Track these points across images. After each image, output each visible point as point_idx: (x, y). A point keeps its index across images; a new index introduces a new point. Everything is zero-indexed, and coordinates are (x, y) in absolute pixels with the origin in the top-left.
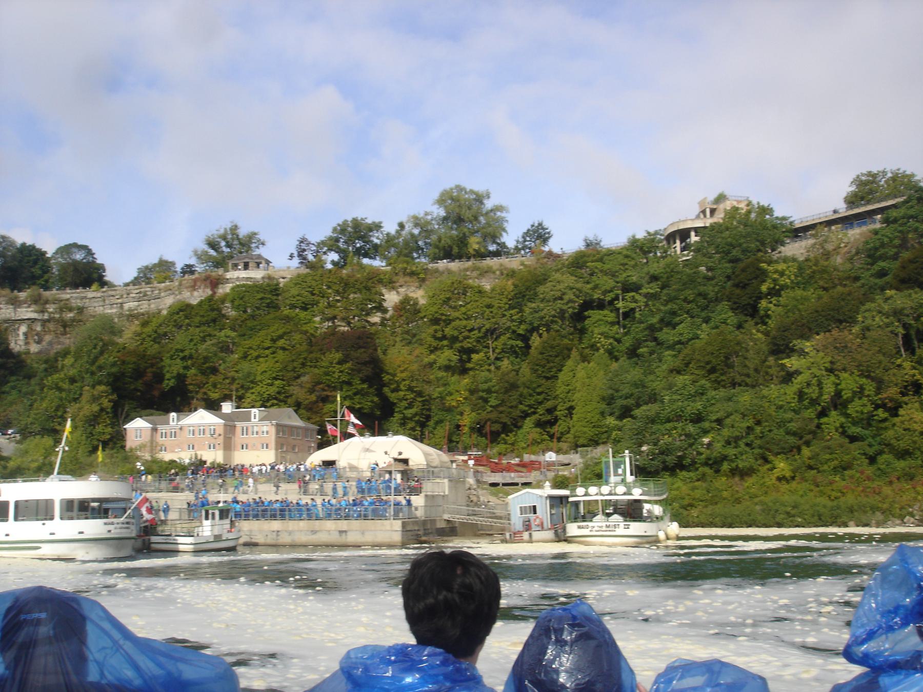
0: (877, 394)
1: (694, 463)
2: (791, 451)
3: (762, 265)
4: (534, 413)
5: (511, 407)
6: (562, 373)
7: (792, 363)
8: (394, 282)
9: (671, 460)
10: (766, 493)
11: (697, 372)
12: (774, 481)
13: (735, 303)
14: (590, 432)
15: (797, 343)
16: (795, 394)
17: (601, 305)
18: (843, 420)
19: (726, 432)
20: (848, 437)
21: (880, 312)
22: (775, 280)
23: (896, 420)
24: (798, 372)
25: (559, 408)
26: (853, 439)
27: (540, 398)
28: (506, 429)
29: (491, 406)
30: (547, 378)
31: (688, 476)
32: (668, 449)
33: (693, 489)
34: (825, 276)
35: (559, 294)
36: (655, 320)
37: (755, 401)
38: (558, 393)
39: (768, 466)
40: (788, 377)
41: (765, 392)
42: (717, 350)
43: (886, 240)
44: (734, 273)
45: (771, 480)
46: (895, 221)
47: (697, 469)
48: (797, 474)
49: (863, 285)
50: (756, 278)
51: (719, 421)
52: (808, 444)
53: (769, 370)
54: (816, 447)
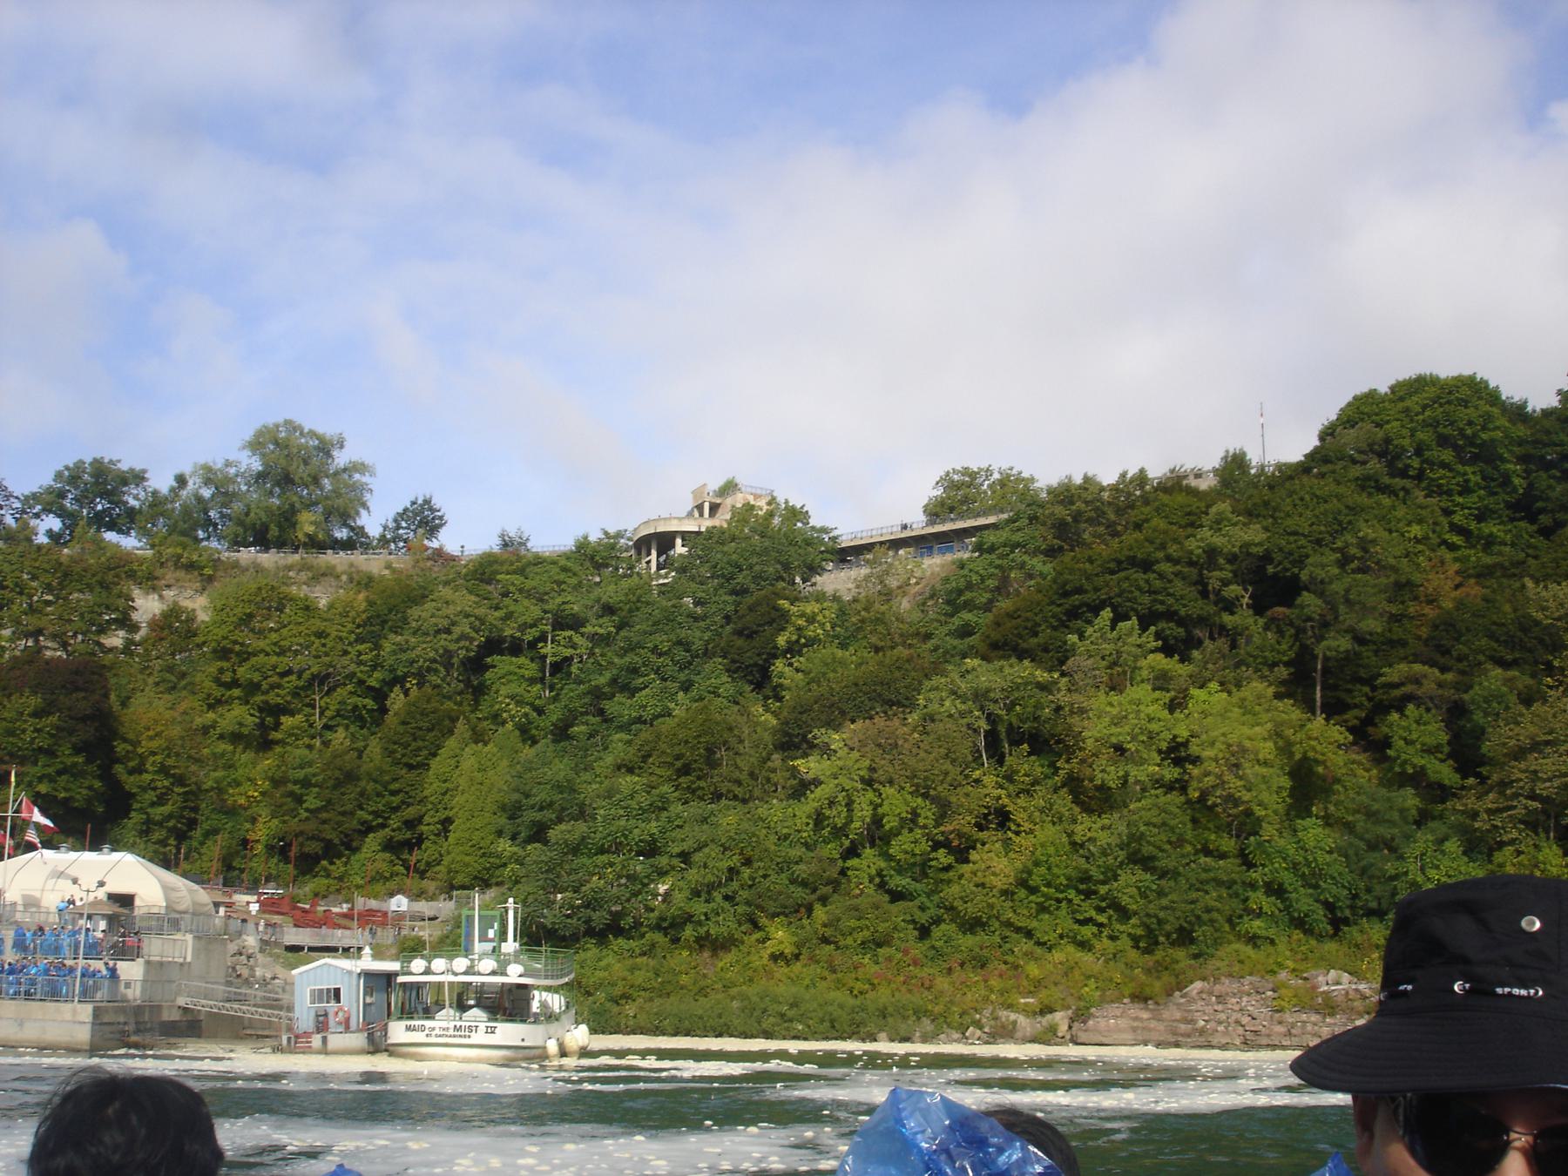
0: (938, 824)
1: (637, 924)
2: (797, 911)
3: (781, 602)
4: (383, 826)
5: (343, 814)
6: (438, 758)
7: (809, 766)
8: (156, 578)
9: (599, 918)
10: (751, 980)
11: (658, 771)
12: (765, 961)
13: (733, 661)
14: (475, 864)
15: (820, 734)
16: (809, 817)
17: (516, 649)
18: (883, 864)
19: (693, 875)
20: (889, 892)
21: (954, 693)
22: (799, 629)
23: (966, 868)
24: (817, 782)
25: (427, 819)
26: (897, 896)
27: (396, 800)
28: (330, 851)
29: (307, 810)
30: (411, 767)
31: (626, 947)
32: (596, 900)
33: (632, 969)
34: (880, 628)
35: (446, 623)
36: (602, 680)
37: (745, 825)
38: (426, 793)
39: (758, 935)
40: (802, 788)
41: (762, 811)
42: (695, 738)
43: (975, 579)
44: (736, 611)
45: (761, 958)
46: (992, 549)
47: (643, 936)
48: (804, 951)
49: (936, 649)
50: (770, 623)
51: (685, 857)
52: (824, 900)
53: (772, 775)
54: (837, 905)
